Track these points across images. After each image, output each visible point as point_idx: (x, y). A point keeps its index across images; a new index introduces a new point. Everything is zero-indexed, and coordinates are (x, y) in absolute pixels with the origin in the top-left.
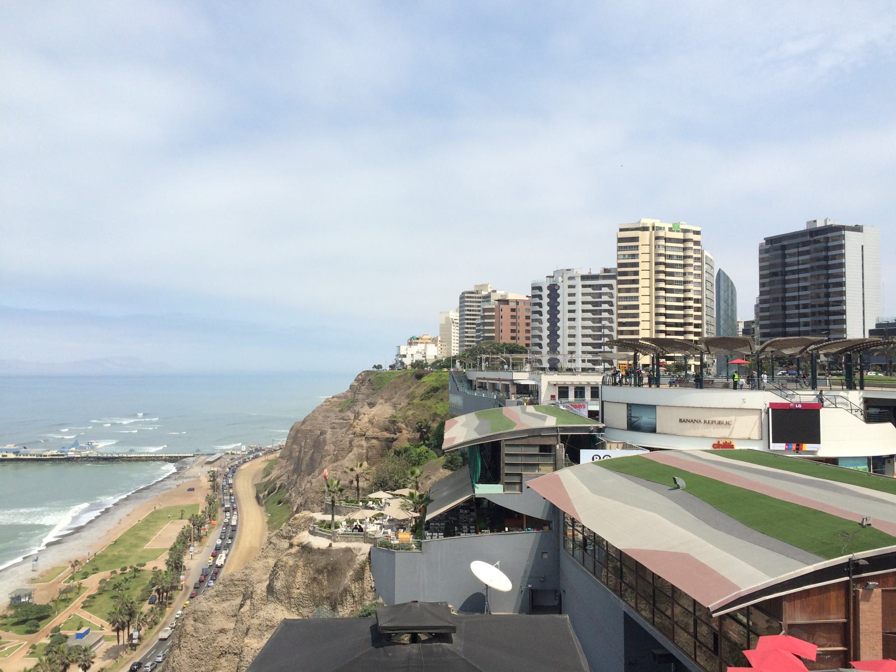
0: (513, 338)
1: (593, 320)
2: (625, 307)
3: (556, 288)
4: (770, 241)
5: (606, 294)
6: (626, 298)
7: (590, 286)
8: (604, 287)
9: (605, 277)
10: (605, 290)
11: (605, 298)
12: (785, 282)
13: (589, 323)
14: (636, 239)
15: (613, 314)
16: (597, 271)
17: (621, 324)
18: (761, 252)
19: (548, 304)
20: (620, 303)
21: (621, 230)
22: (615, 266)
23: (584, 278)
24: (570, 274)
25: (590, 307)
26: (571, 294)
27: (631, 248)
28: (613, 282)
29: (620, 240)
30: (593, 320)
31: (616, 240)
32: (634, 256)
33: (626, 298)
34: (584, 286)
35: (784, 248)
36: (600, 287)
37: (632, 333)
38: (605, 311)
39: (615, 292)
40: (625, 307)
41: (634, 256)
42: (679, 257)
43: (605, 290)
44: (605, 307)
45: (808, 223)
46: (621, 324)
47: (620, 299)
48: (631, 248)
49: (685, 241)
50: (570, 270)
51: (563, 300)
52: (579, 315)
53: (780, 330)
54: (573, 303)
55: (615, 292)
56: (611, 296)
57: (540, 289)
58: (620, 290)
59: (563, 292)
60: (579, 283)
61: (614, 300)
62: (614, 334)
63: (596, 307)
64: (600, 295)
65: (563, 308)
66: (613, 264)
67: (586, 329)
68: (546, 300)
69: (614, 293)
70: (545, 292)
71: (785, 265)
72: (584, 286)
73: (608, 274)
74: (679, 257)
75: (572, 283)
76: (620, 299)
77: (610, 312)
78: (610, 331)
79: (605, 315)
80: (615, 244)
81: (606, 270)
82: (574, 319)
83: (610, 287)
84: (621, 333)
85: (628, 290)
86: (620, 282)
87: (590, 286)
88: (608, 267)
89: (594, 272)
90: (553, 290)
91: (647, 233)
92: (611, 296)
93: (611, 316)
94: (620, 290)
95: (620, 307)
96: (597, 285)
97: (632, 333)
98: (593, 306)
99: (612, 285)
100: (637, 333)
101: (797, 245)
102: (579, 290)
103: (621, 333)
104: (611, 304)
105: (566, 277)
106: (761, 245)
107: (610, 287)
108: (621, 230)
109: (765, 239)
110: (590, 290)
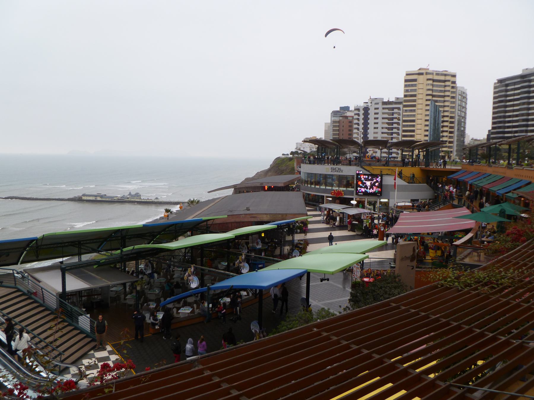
0: (349, 138)
4: (500, 81)
5: (396, 113)
10: (396, 111)
11: (395, 116)
14: (415, 80)
16: (392, 99)
20: (404, 119)
22: (403, 96)
23: (384, 103)
24: (376, 101)
25: (387, 121)
28: (401, 106)
30: (388, 129)
31: (404, 81)
34: (383, 108)
35: (507, 85)
36: (393, 109)
43: (396, 111)
44: (395, 121)
46: (404, 131)
49: (445, 81)
50: (377, 99)
51: (371, 116)
54: (377, 118)
56: (399, 114)
57: (358, 110)
59: (372, 112)
60: (380, 106)
61: (401, 117)
62: (400, 137)
64: (393, 114)
65: (371, 121)
66: (401, 95)
68: (362, 116)
69: (401, 114)
70: (362, 112)
72: (383, 108)
73: (398, 102)
75: (377, 106)
80: (403, 83)
81: (398, 98)
82: (377, 128)
83: (399, 109)
86: (405, 106)
89: (390, 100)
91: (421, 76)
101: (515, 84)
102: (380, 111)
104: (399, 119)
105: (373, 103)
107: (399, 109)
109: (497, 80)
110: (387, 111)
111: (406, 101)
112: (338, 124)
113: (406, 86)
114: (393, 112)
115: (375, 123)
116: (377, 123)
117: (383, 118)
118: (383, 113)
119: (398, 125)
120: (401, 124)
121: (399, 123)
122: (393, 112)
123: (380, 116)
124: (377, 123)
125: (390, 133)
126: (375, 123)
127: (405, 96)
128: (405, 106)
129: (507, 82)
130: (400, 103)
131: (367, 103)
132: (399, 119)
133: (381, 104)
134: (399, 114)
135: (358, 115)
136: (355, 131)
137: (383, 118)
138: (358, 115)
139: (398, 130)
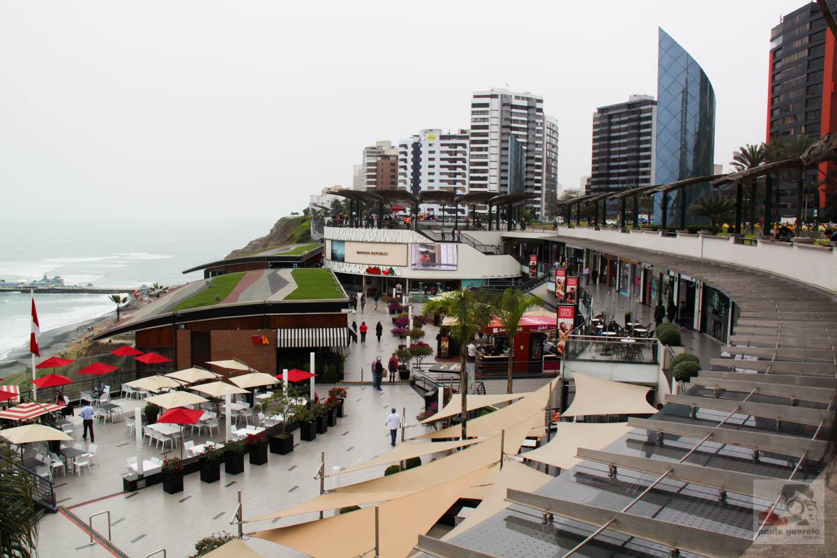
1: (450, 175)
2: (476, 164)
3: (419, 145)
4: (601, 110)
5: (460, 152)
6: (477, 156)
9: (460, 138)
10: (460, 148)
11: (459, 156)
12: (610, 146)
13: (446, 177)
14: (487, 105)
15: (465, 170)
16: (455, 132)
17: (472, 179)
18: (595, 119)
20: (472, 160)
21: (476, 97)
22: (470, 128)
23: (442, 137)
25: (446, 163)
27: (483, 112)
28: (467, 142)
29: (474, 105)
30: (450, 175)
31: (471, 106)
32: (484, 120)
33: (477, 156)
34: (442, 145)
35: (610, 117)
36: (455, 146)
37: (481, 186)
38: (459, 166)
39: (467, 150)
40: (476, 164)
41: (484, 120)
42: (523, 122)
43: (460, 148)
44: (460, 163)
45: (630, 97)
46: (472, 179)
47: (472, 156)
48: (483, 112)
51: (424, 156)
52: (437, 170)
53: (604, 186)
55: (467, 150)
57: (405, 146)
58: (472, 149)
59: (424, 150)
60: (437, 142)
61: (467, 158)
62: (467, 187)
63: (452, 163)
64: (456, 153)
65: (424, 163)
68: (410, 157)
69: (467, 154)
70: (410, 149)
71: (610, 131)
73: (463, 135)
74: (523, 122)
76: (472, 156)
77: (464, 168)
80: (470, 109)
81: (463, 131)
82: (433, 174)
83: (464, 146)
84: (472, 186)
85: (480, 149)
86: (473, 142)
88: (463, 128)
90: (417, 147)
91: (494, 100)
93: (464, 171)
94: (472, 149)
95: (472, 164)
96: (453, 144)
97: (481, 186)
98: (450, 162)
100: (485, 186)
103: (472, 186)
104: (464, 160)
106: (595, 114)
107: (464, 146)
108: (476, 97)
110: (447, 148)
111: (473, 135)
112: (375, 167)
113: (473, 113)
114: (454, 186)
116: (433, 166)
117: (442, 159)
119: (463, 169)
120: (467, 168)
124: (433, 166)
125: (452, 181)
126: (430, 167)
127: (473, 127)
128: (473, 142)
129: (611, 113)
130: (467, 138)
132: (464, 160)
135: (405, 153)
136: (400, 177)
138: (405, 153)
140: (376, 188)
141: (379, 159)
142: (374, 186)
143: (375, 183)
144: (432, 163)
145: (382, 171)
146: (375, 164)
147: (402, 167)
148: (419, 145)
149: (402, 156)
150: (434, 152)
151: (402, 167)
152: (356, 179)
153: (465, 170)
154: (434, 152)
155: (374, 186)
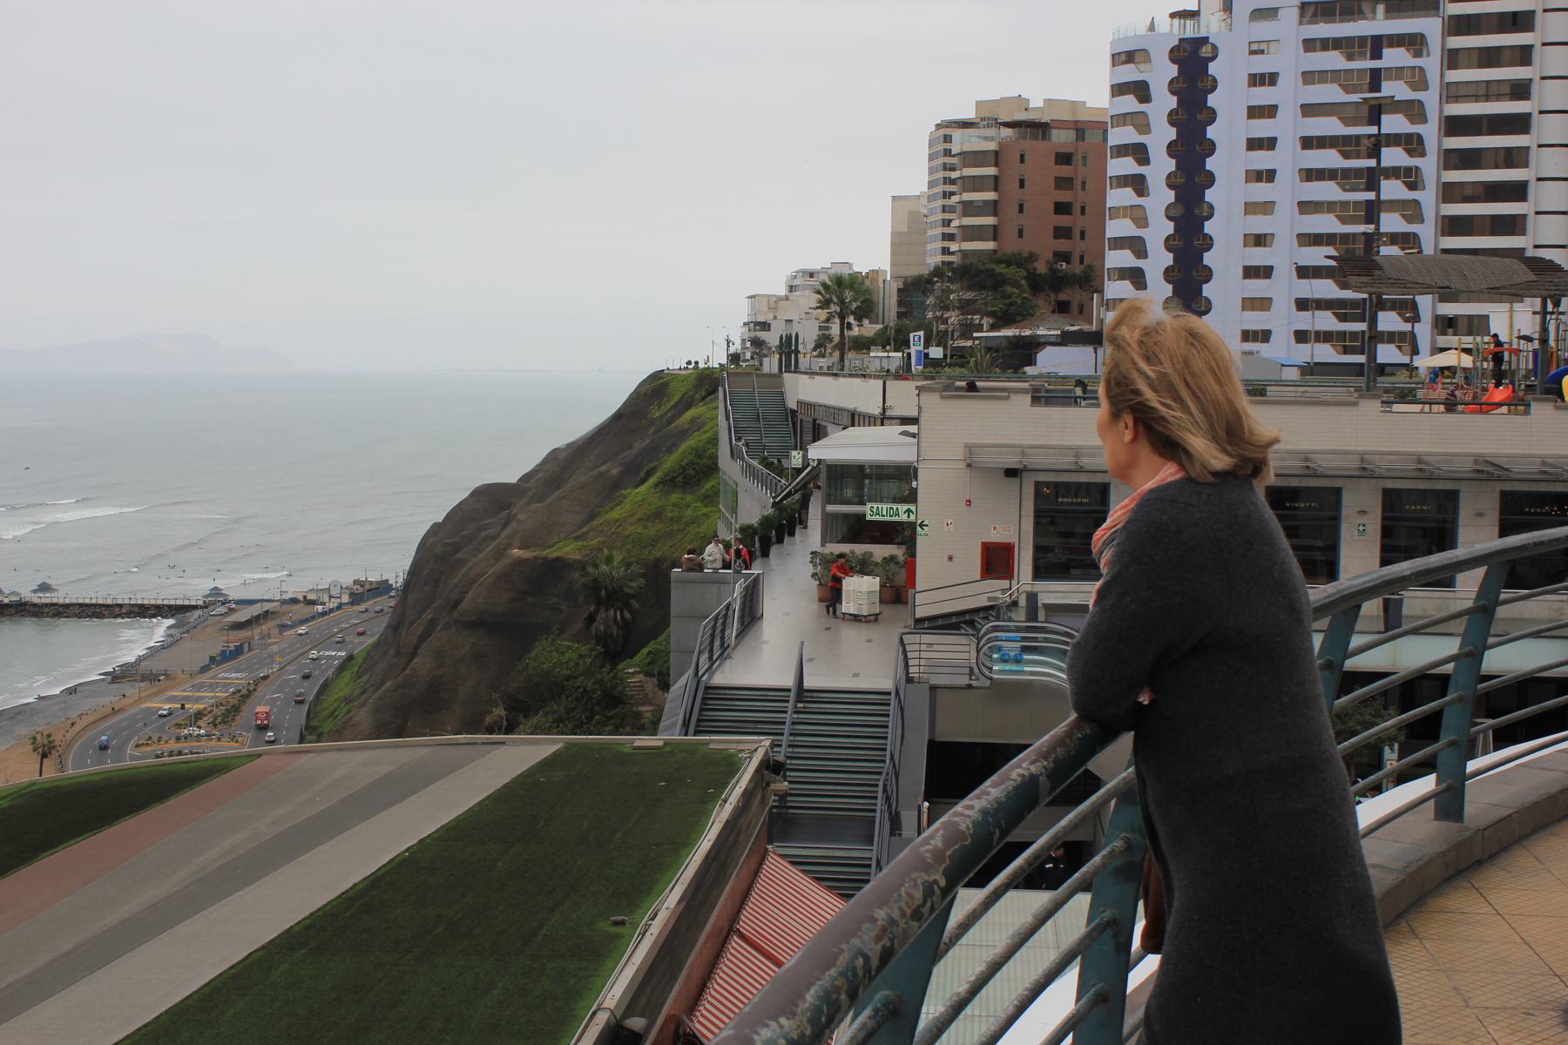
3: (1205, 51)
7: (1326, 44)
8: (1391, 45)
10: (1394, 57)
15: (1423, 154)
17: (1450, 193)
19: (1173, 118)
26: (1262, 76)
34: (1310, 45)
36: (1376, 45)
47: (1453, 93)
52: (1287, 159)
56: (1419, 81)
59: (1230, 71)
67: (1316, 212)
70: (1162, 73)
77: (1413, 144)
78: (1409, 219)
79: (1393, 157)
83: (1415, 43)
84: (1454, 226)
87: (1326, 44)
92: (1419, 81)
94: (1453, 59)
99: (1422, 36)
100: (1512, 225)
103: (1454, 226)
107: (1415, 43)
110: (1334, 60)
112: (990, 221)
115: (1255, 112)
117: (1308, 143)
118: (1309, 110)
120: (1431, 144)
121: (1416, 203)
122: (1375, 64)
123: (1288, 127)
124: (1269, 111)
125: (1357, 172)
131: (1193, 15)
132: (1415, 111)
133: (1295, 12)
134: (1418, 80)
135: (1141, 91)
136: (1117, 228)
137: (1308, 143)
138: (1141, 91)
139: (1412, 186)
140: (995, 252)
141: (1007, 133)
142: (990, 245)
143: (995, 234)
144: (1262, 128)
145: (1022, 184)
146: (996, 157)
147: (1122, 151)
148: (1205, 51)
149: (1120, 136)
150: (1270, 79)
151: (1122, 151)
152: (900, 244)
153: (1423, 154)
154: (1270, 79)
155: (990, 245)
